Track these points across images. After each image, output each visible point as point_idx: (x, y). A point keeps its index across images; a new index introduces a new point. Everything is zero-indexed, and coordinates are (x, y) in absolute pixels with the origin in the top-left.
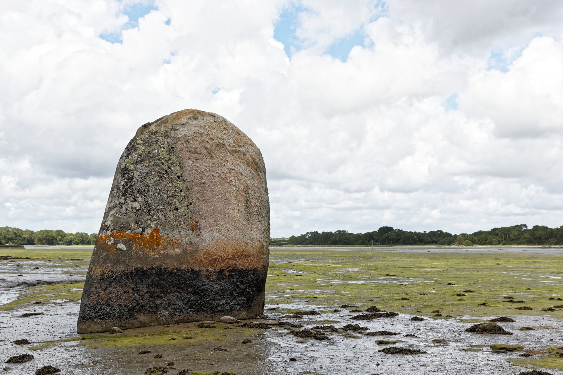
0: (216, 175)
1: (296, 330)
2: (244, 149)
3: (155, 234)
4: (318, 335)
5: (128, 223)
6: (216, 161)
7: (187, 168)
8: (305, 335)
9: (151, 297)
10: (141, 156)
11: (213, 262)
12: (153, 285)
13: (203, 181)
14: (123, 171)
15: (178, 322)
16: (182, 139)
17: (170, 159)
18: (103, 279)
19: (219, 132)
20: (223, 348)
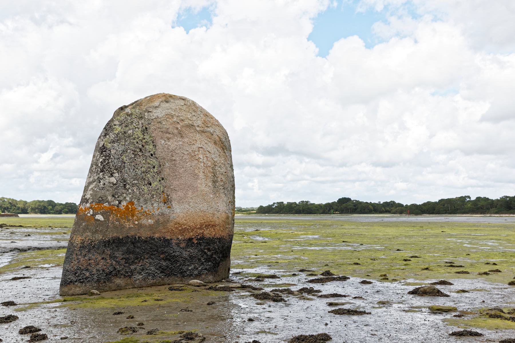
1: (256, 292)
2: (211, 130)
3: (130, 207)
4: (276, 298)
5: (105, 196)
6: (186, 140)
7: (159, 146)
8: (265, 297)
9: (126, 263)
10: (117, 135)
11: (183, 231)
12: (129, 252)
13: (174, 158)
14: (102, 150)
15: (151, 285)
16: (155, 120)
17: (144, 139)
18: (83, 247)
20: (190, 309)
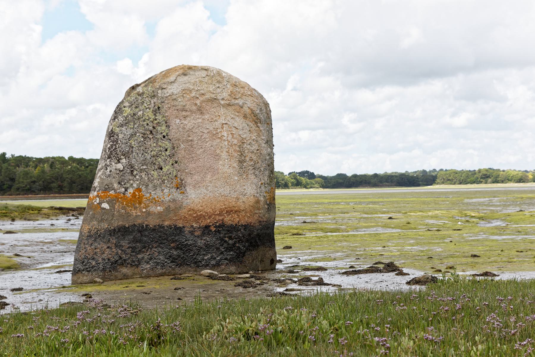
0: (206, 131)
2: (240, 102)
3: (137, 194)
5: (111, 184)
7: (173, 126)
10: (126, 118)
11: (198, 218)
12: (135, 240)
14: (111, 134)
16: (169, 97)
18: (90, 236)
19: (211, 86)
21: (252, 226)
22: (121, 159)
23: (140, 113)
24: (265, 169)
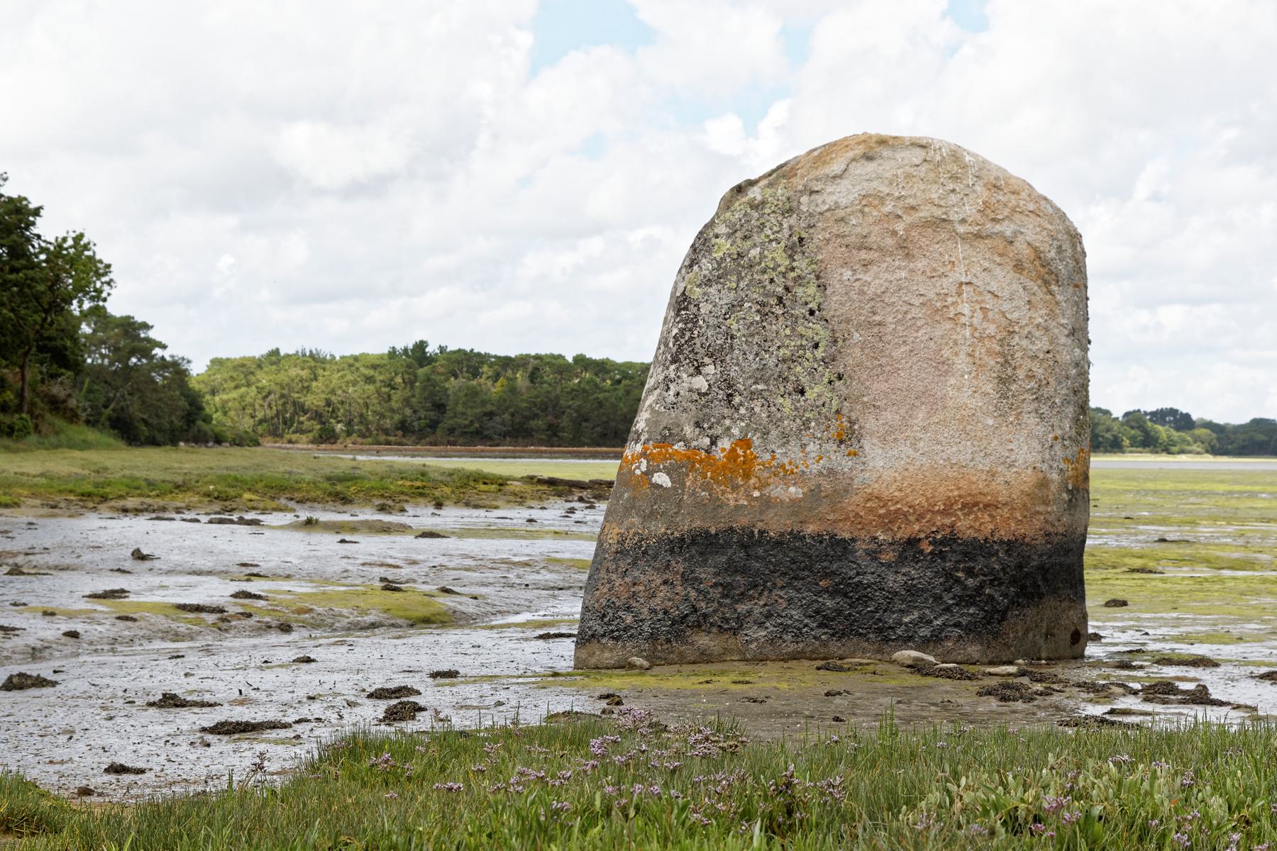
0: (917, 301)
2: (1007, 229)
3: (740, 452)
6: (920, 264)
7: (835, 286)
10: (719, 264)
11: (890, 520)
14: (681, 303)
16: (828, 214)
18: (621, 552)
21: (1028, 545)
22: (704, 365)
23: (755, 252)
24: (1066, 402)
